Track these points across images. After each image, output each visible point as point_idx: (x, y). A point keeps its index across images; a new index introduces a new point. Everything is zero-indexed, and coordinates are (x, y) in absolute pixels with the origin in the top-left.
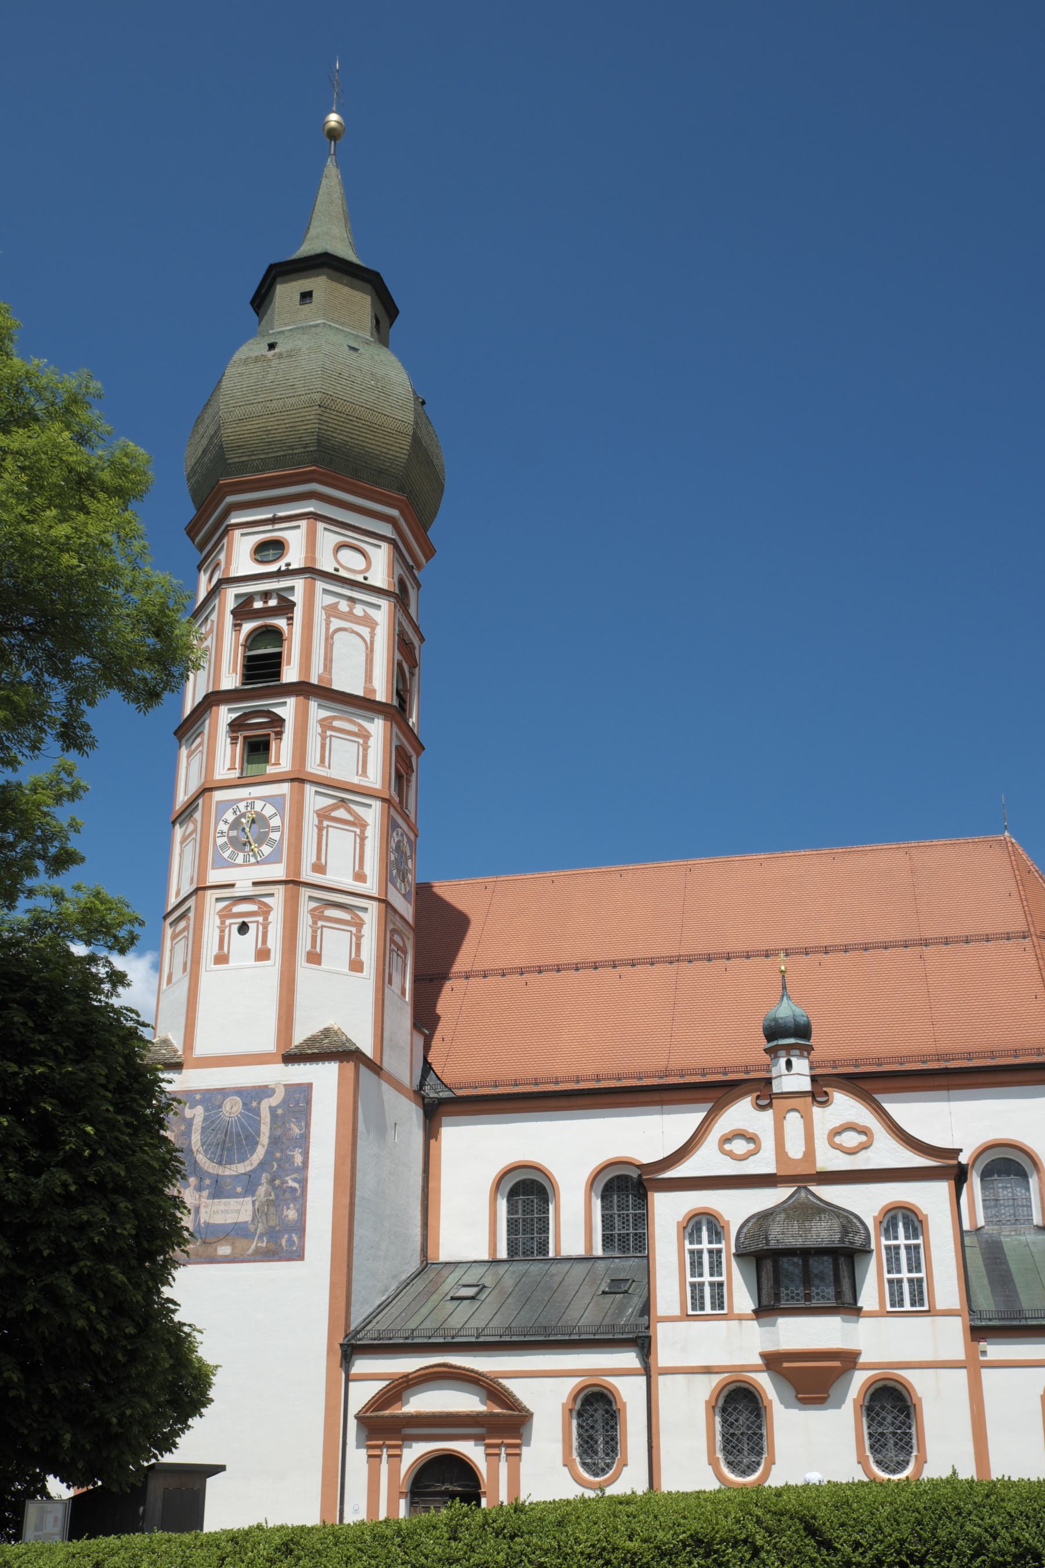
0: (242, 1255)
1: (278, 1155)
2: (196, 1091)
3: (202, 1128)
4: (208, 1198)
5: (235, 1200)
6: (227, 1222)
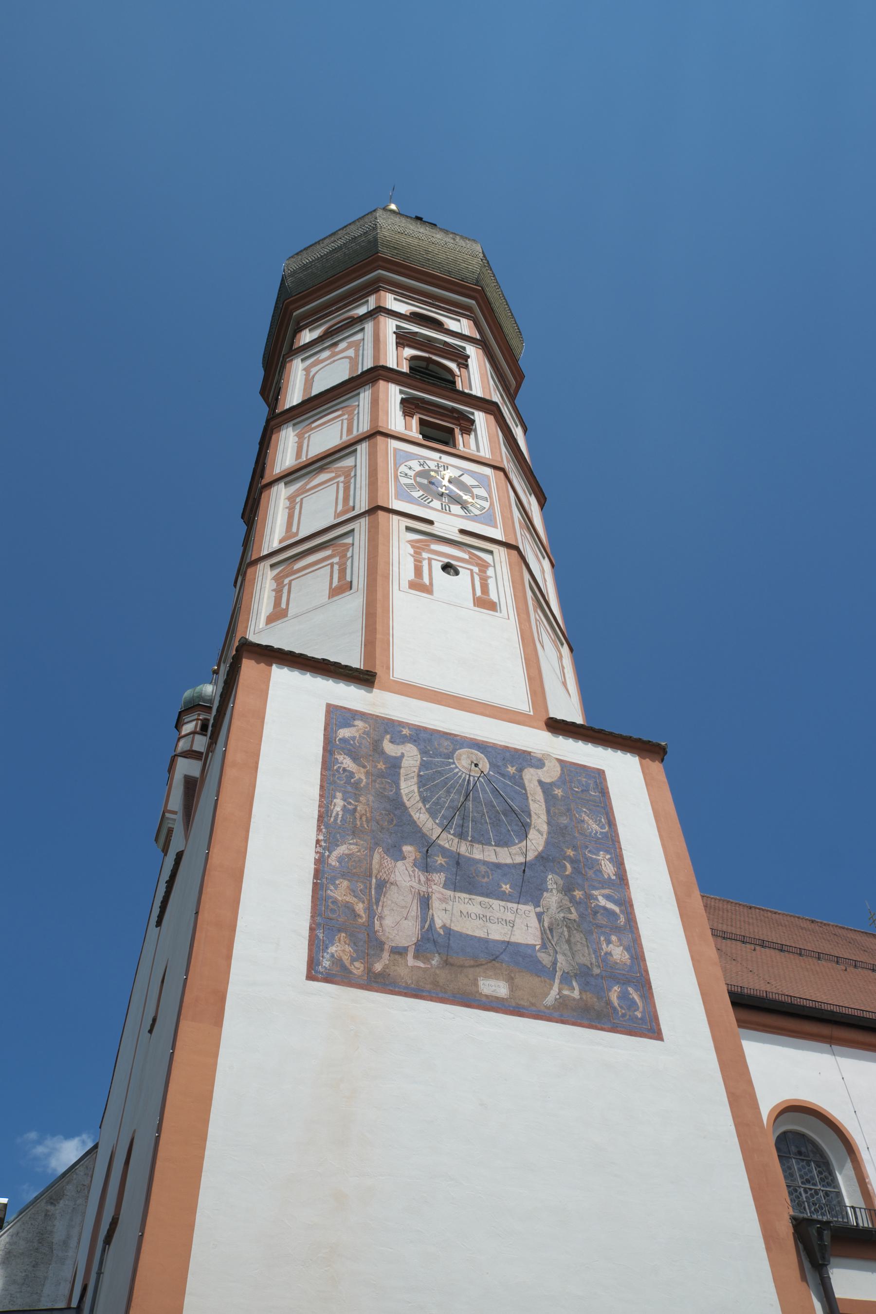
0: (533, 1004)
1: (570, 853)
2: (401, 724)
3: (419, 776)
4: (445, 886)
5: (503, 903)
6: (491, 937)
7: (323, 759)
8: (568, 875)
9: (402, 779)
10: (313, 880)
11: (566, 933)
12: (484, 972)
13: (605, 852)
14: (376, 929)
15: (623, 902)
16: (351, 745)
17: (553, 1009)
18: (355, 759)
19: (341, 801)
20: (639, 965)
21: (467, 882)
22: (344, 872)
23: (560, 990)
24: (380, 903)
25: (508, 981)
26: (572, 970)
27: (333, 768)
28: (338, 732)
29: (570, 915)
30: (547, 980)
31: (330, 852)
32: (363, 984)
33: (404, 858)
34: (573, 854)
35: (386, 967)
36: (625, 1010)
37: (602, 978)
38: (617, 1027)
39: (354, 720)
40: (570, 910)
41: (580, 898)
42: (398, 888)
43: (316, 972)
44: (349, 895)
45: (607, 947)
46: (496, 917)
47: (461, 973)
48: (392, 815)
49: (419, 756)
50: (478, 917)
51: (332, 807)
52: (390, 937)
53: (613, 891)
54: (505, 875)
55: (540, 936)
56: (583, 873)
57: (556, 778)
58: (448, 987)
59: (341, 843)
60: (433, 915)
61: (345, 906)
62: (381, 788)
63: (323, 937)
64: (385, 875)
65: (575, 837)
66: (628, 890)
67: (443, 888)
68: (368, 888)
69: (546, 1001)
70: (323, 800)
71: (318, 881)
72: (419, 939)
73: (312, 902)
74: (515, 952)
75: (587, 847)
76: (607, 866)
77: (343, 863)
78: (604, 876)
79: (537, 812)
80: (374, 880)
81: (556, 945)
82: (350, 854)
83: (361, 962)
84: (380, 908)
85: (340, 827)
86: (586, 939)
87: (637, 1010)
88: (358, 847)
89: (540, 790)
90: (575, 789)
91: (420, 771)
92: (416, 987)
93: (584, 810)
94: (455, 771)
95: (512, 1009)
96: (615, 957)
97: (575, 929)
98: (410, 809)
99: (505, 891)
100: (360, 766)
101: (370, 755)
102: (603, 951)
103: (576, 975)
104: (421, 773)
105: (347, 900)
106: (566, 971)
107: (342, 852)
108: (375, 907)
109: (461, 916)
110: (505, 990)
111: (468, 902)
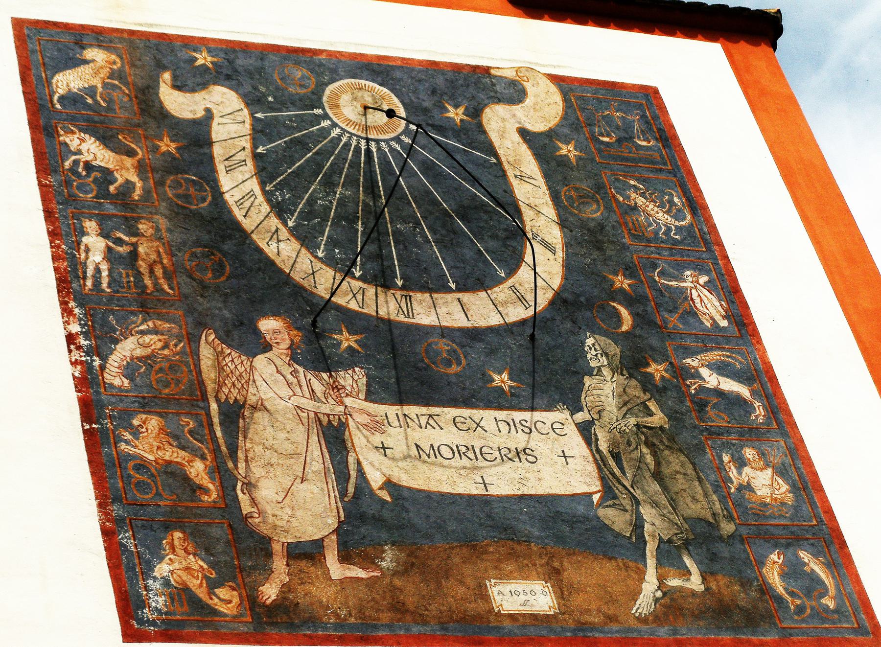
0: (611, 619)
1: (622, 282)
3: (256, 156)
4: (371, 397)
5: (502, 415)
6: (493, 491)
7: (35, 150)
8: (627, 332)
9: (221, 168)
10: (83, 426)
11: (649, 459)
12: (496, 568)
13: (694, 269)
14: (244, 513)
15: (754, 372)
16: (89, 107)
17: (654, 621)
18: (107, 139)
19: (100, 239)
20: (812, 504)
21: (416, 379)
22: (144, 398)
23: (661, 579)
24: (241, 454)
25: (550, 579)
26: (677, 534)
27: (63, 167)
28: (54, 81)
29: (649, 419)
30: (631, 564)
31: (104, 359)
32: (247, 633)
33: (267, 347)
34: (629, 285)
35: (286, 589)
36: (800, 598)
37: (742, 541)
38: (791, 635)
39: (84, 49)
40: (647, 408)
41: (662, 377)
42: (271, 415)
43: (141, 621)
44: (167, 446)
45: (740, 473)
46: (495, 446)
47: (448, 578)
48: (219, 255)
49: (246, 112)
50: (457, 451)
51: (83, 256)
52: (278, 523)
53: (728, 354)
54: (492, 352)
55: (595, 474)
56: (659, 322)
57: (558, 119)
58: (427, 610)
59: (121, 334)
60: (359, 463)
61: (166, 473)
62: (178, 196)
63: (136, 545)
64: (235, 392)
65: (625, 247)
66: (759, 346)
67: (365, 400)
68: (205, 424)
69: (637, 606)
70: (57, 242)
71: (94, 426)
72: (342, 518)
73: (93, 473)
74: (551, 515)
75: (654, 266)
76: (706, 301)
77: (138, 379)
78: (703, 323)
79: (532, 201)
80: (214, 407)
81: (632, 487)
82: (148, 357)
83: (230, 587)
84: (242, 465)
85: (111, 299)
86: (693, 464)
87: (824, 593)
88: (161, 337)
89: (529, 152)
90: (601, 138)
91: (255, 147)
92: (359, 621)
93: (632, 182)
94: (333, 135)
95: (569, 634)
96: (759, 493)
97: (667, 446)
98: (254, 236)
99: (500, 389)
100: (122, 154)
101: (138, 125)
102: (732, 482)
103: (687, 544)
104: (259, 150)
105: (167, 458)
106: (666, 538)
107: (128, 354)
108: (230, 465)
109: (420, 457)
110: (548, 598)
111: (428, 423)
